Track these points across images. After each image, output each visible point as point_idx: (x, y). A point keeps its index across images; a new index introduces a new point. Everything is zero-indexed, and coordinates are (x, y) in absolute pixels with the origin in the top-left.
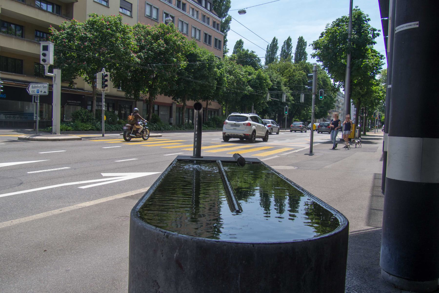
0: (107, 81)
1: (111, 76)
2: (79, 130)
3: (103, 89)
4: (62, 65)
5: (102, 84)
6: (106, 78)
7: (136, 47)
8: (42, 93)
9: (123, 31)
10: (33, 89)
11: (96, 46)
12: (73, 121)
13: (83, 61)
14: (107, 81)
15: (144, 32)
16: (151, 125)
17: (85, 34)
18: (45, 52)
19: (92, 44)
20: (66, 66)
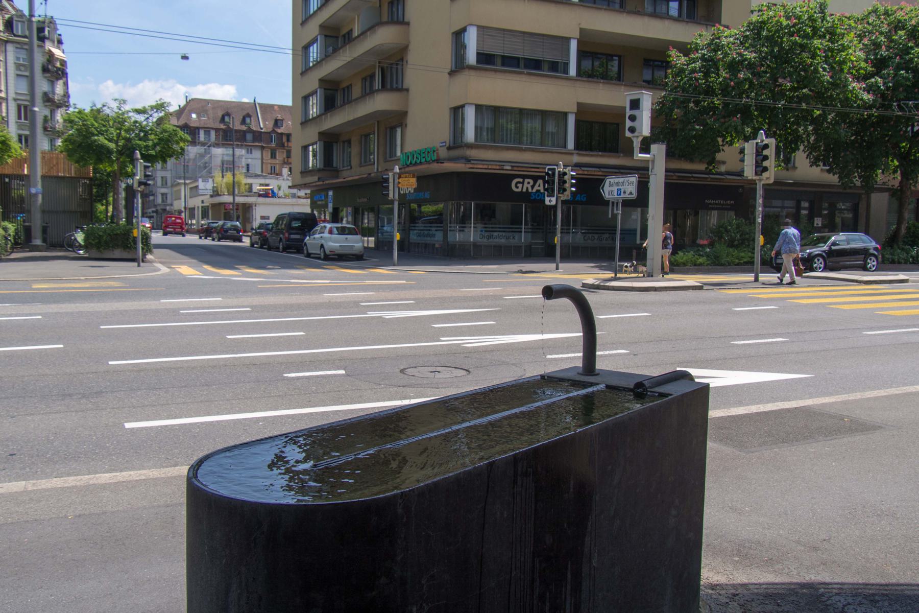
0: (766, 158)
1: (777, 147)
2: (722, 265)
3: (757, 178)
4: (689, 127)
5: (756, 167)
6: (765, 152)
7: (863, 64)
8: (627, 196)
9: (830, 34)
10: (612, 189)
11: (762, 77)
12: (711, 245)
13: (732, 114)
14: (766, 158)
15: (888, 25)
16: (903, 249)
17: (740, 55)
18: (634, 112)
19: (754, 74)
20: (697, 130)
